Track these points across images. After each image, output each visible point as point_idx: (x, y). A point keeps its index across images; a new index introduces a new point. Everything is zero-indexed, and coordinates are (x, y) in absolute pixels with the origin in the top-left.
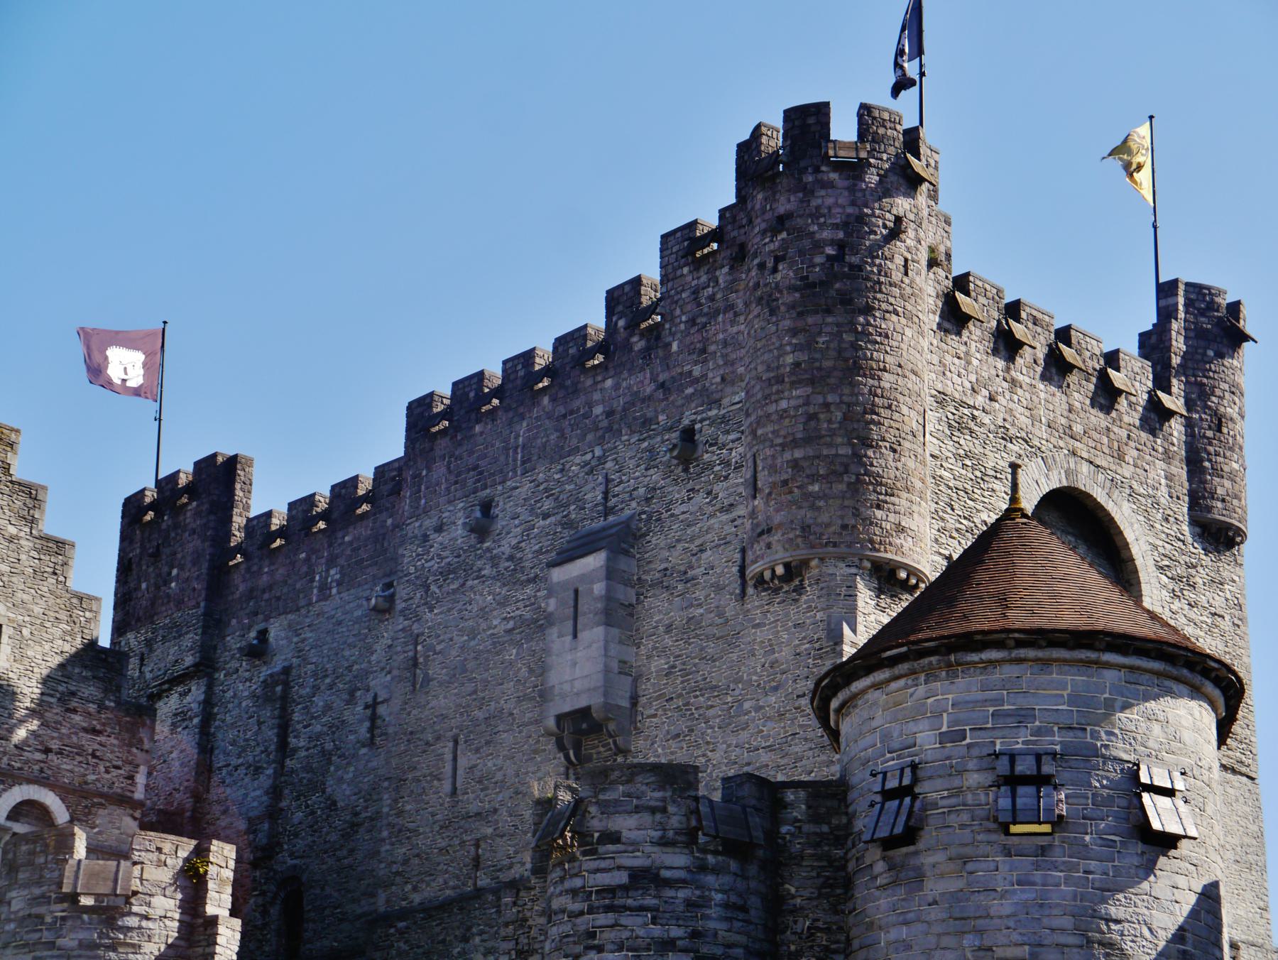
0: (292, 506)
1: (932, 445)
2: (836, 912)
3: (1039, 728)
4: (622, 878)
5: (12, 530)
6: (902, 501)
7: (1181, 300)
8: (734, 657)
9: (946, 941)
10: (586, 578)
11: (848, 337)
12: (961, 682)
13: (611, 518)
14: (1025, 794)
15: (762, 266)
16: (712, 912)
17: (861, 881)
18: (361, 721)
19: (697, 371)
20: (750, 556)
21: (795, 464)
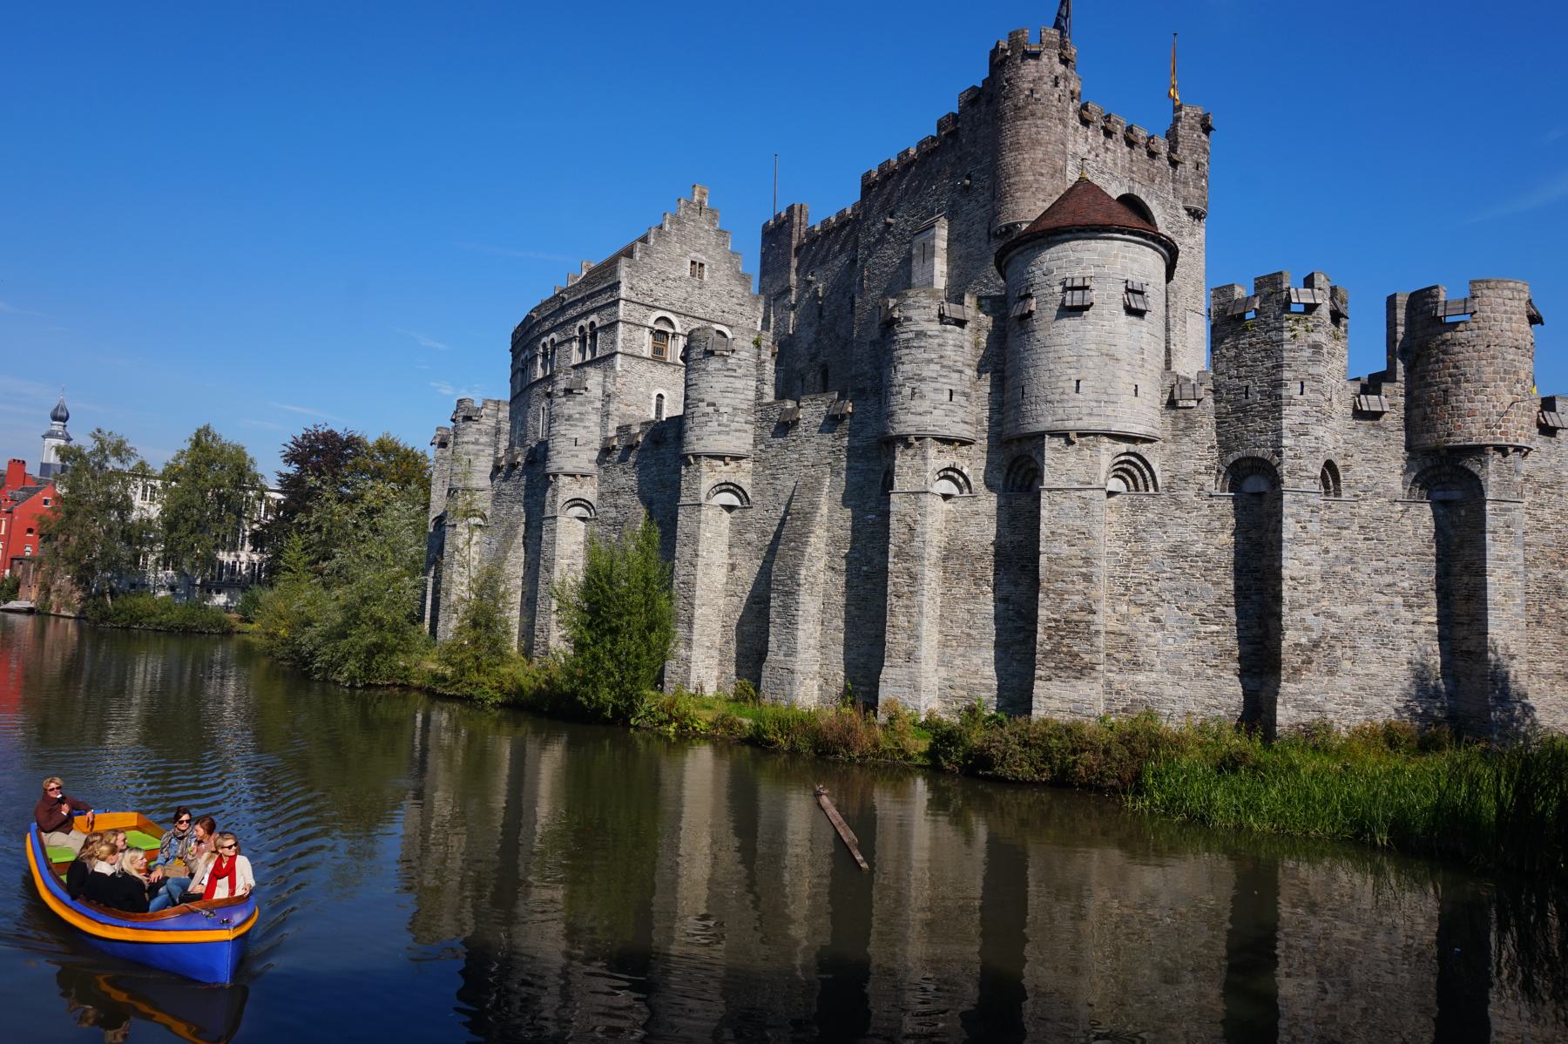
0: (822, 223)
4: (911, 335)
5: (707, 227)
7: (1183, 113)
11: (1034, 130)
14: (1078, 294)
16: (949, 348)
17: (1010, 335)
19: (972, 150)
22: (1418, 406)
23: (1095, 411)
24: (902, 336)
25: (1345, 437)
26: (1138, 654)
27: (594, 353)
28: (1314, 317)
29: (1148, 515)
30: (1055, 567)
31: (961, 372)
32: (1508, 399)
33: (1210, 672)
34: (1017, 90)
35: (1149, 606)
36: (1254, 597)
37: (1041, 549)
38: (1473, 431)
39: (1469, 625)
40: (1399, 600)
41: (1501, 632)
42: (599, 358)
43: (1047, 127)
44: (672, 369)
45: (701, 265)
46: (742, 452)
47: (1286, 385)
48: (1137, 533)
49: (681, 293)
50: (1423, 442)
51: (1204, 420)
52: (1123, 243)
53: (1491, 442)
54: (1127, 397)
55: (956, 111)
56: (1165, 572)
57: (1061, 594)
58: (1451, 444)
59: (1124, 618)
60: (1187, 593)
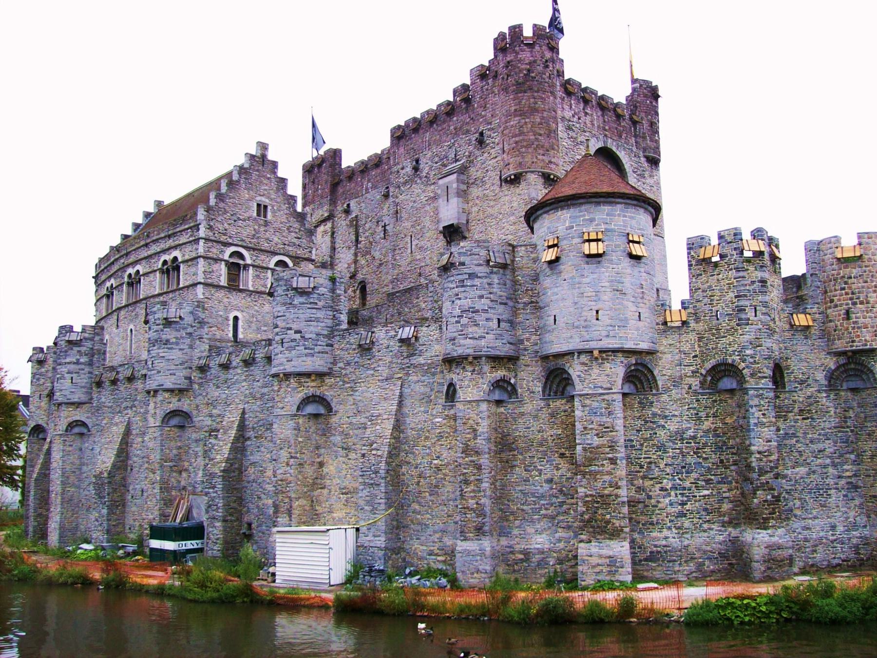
0: (355, 164)
1: (560, 134)
5: (269, 176)
6: (552, 152)
8: (499, 205)
10: (451, 182)
11: (532, 100)
12: (572, 210)
13: (458, 163)
14: (593, 244)
15: (503, 78)
18: (381, 232)
20: (503, 173)
21: (516, 143)
22: (831, 321)
23: (611, 334)
24: (460, 277)
27: (178, 283)
29: (653, 409)
33: (705, 526)
34: (517, 70)
36: (732, 468)
37: (577, 441)
39: (874, 476)
40: (828, 461)
42: (182, 289)
43: (542, 98)
44: (244, 295)
45: (266, 207)
46: (325, 370)
47: (745, 310)
48: (646, 422)
49: (249, 231)
50: (836, 347)
54: (633, 323)
55: (468, 82)
56: (669, 452)
58: (854, 348)
59: (639, 489)
60: (684, 467)
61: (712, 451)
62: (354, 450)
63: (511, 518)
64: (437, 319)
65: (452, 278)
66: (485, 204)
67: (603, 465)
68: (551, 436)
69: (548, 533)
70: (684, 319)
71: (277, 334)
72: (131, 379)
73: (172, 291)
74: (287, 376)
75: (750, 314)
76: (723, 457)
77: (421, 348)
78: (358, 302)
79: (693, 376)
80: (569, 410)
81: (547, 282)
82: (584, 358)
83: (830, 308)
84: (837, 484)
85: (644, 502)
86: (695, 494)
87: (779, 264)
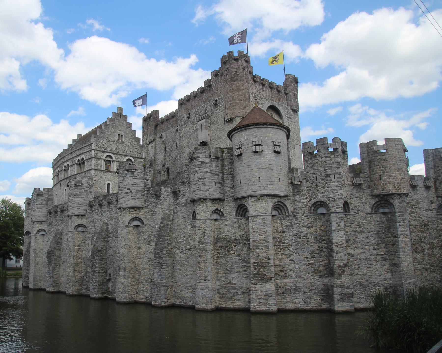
2: (232, 166)
3: (259, 137)
4: (200, 163)
9: (246, 169)
14: (257, 147)
17: (235, 161)
22: (372, 181)
23: (266, 188)
25: (350, 192)
26: (286, 273)
28: (337, 153)
29: (286, 223)
30: (255, 244)
31: (218, 175)
32: (400, 177)
33: (311, 277)
35: (289, 256)
36: (324, 250)
37: (250, 238)
38: (390, 189)
39: (394, 254)
40: (372, 247)
41: (405, 257)
46: (141, 206)
47: (329, 176)
48: (283, 229)
50: (375, 193)
51: (303, 189)
52: (271, 129)
53: (396, 192)
56: (294, 243)
57: (258, 253)
59: (281, 260)
60: (301, 250)
61: (314, 242)
62: (153, 241)
63: (222, 273)
64: (189, 182)
65: (194, 164)
66: (218, 132)
67: (262, 249)
68: (240, 235)
69: (238, 280)
70: (301, 181)
71: (120, 190)
72: (62, 211)
73: (82, 173)
74: (124, 208)
75: (332, 177)
76: (320, 245)
77: (182, 195)
78: (166, 177)
79: (305, 207)
80: (248, 223)
81: (237, 164)
82: (253, 199)
83: (372, 174)
84: (376, 258)
85: (282, 266)
86: (307, 262)
87: (347, 154)
